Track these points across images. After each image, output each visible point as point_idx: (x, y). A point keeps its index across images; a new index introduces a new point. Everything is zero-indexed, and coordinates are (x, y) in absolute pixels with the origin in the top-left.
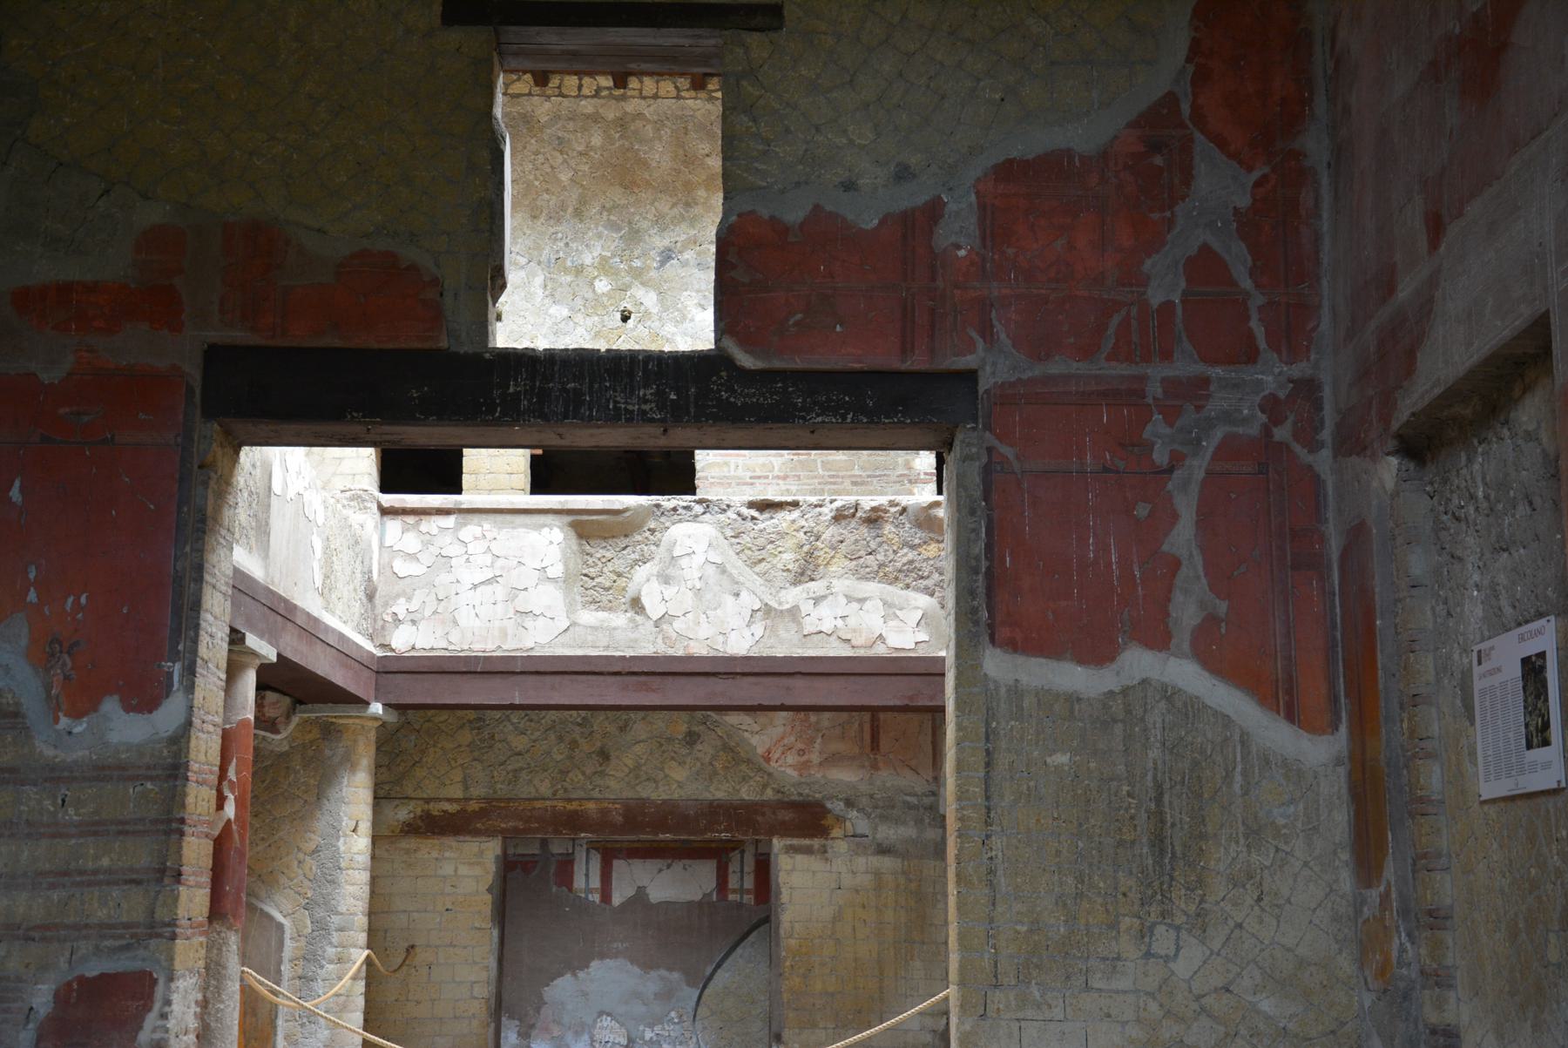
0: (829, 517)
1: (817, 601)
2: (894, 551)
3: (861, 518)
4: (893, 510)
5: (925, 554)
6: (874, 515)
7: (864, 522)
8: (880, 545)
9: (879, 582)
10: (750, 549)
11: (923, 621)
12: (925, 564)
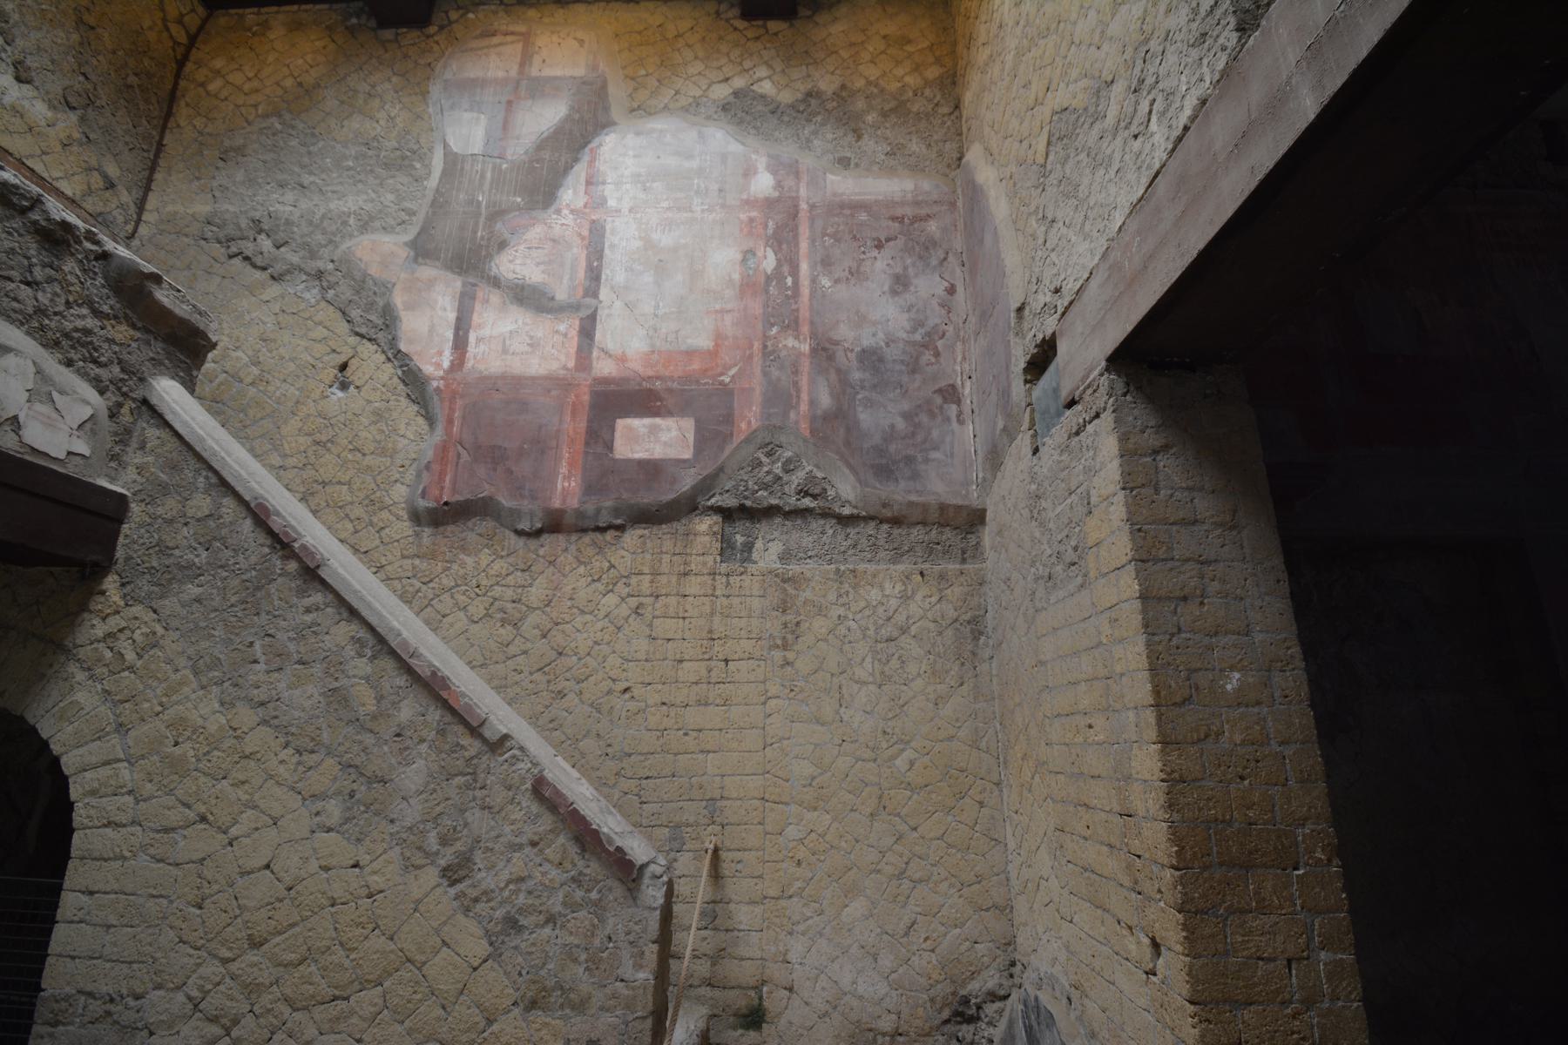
2: (67, 302)
3: (35, 223)
4: (88, 245)
5: (110, 332)
6: (60, 233)
8: (50, 280)
9: (28, 333)
11: (88, 426)
12: (106, 346)
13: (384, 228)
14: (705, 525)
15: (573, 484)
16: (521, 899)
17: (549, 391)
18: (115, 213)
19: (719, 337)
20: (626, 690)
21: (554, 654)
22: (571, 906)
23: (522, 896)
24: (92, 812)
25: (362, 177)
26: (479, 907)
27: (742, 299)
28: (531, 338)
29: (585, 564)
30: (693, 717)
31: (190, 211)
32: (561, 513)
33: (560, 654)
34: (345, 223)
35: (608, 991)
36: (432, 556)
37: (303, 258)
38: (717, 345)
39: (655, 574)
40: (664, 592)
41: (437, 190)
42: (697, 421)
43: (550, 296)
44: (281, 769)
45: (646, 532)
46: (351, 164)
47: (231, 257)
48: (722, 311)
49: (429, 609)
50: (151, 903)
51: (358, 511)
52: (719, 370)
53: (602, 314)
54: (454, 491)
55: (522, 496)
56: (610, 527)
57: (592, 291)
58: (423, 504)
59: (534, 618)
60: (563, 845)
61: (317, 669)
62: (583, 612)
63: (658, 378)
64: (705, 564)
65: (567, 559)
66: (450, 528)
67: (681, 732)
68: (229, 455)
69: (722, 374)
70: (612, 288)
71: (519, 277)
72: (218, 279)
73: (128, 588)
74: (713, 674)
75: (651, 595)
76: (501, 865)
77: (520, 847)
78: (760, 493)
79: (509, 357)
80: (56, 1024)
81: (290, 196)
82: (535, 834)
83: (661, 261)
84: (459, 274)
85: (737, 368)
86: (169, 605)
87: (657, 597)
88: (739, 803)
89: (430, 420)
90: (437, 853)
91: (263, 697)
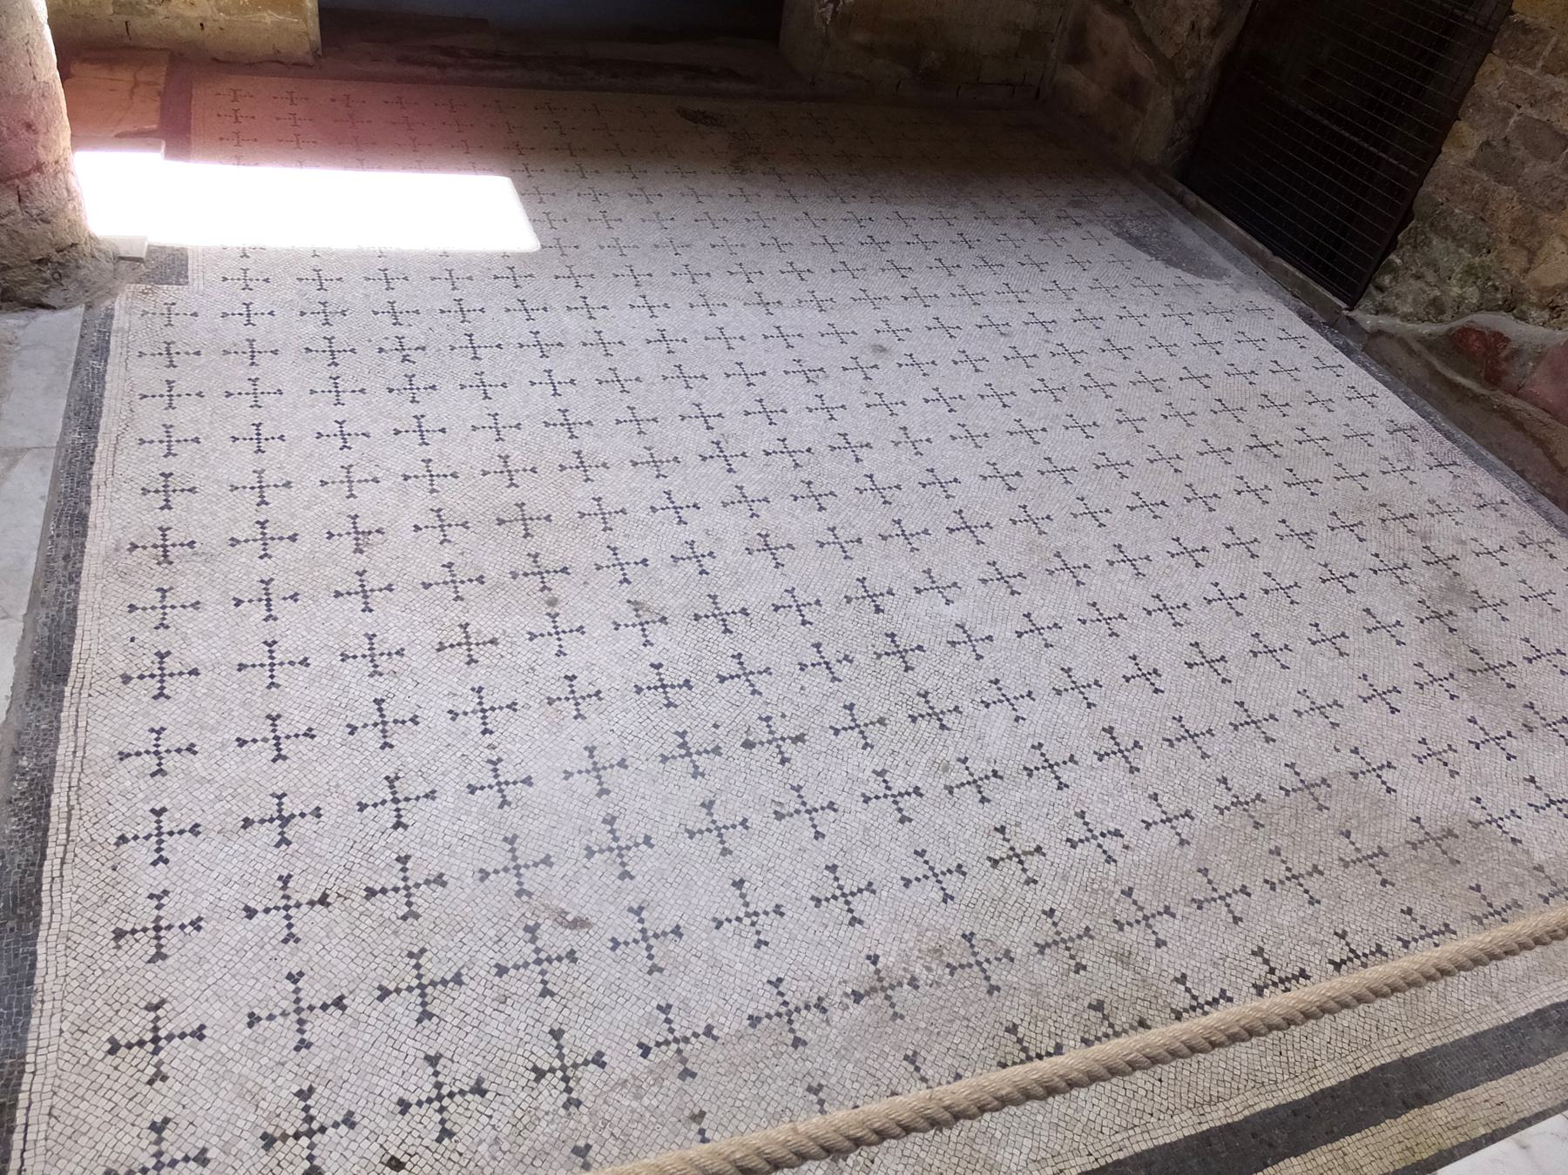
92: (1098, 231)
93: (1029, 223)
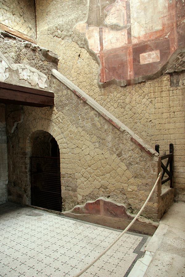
0: (24, 45)
1: (23, 69)
3: (31, 49)
4: (38, 49)
7: (32, 50)
8: (35, 58)
10: (3, 48)
12: (45, 66)
13: (81, 20)
14: (166, 78)
15: (132, 73)
16: (131, 160)
17: (123, 51)
18: (33, 34)
19: (164, 25)
20: (150, 121)
21: (133, 114)
22: (141, 161)
23: (131, 159)
24: (61, 146)
25: (74, 9)
26: (124, 161)
27: (169, 11)
28: (117, 38)
29: (137, 92)
30: (167, 126)
31: (45, 29)
32: (130, 80)
33: (135, 114)
34: (73, 21)
35: (149, 175)
36: (104, 95)
37: (67, 33)
38: (163, 27)
39: (154, 92)
40: (157, 97)
41: (90, 6)
42: (160, 51)
43: (119, 26)
44: (88, 138)
45: (151, 82)
46: (71, 6)
47: (54, 37)
48: (164, 17)
49: (106, 106)
50: (73, 160)
51: (88, 87)
52: (165, 34)
53: (132, 27)
54: (106, 79)
55: (121, 78)
56: (142, 82)
57: (129, 21)
58: (100, 83)
59: (128, 106)
60: (138, 150)
61: (90, 120)
62: (138, 104)
63: (149, 41)
64: (166, 88)
65: (133, 92)
66: (107, 88)
67: (164, 130)
68: (67, 82)
69: (166, 36)
70: (134, 19)
71: (111, 23)
72: (53, 42)
73: (58, 109)
74: (171, 116)
75: (154, 98)
76: (127, 154)
77: (130, 151)
78: (180, 67)
79: (112, 44)
80: (64, 178)
81: (61, 19)
82: (133, 148)
83: (145, 7)
84: (98, 26)
85: (169, 33)
86: (64, 111)
87: (155, 98)
88: (179, 145)
89: (98, 63)
90: (116, 152)
91: (82, 126)
92: (23, 216)
93: (13, 219)
